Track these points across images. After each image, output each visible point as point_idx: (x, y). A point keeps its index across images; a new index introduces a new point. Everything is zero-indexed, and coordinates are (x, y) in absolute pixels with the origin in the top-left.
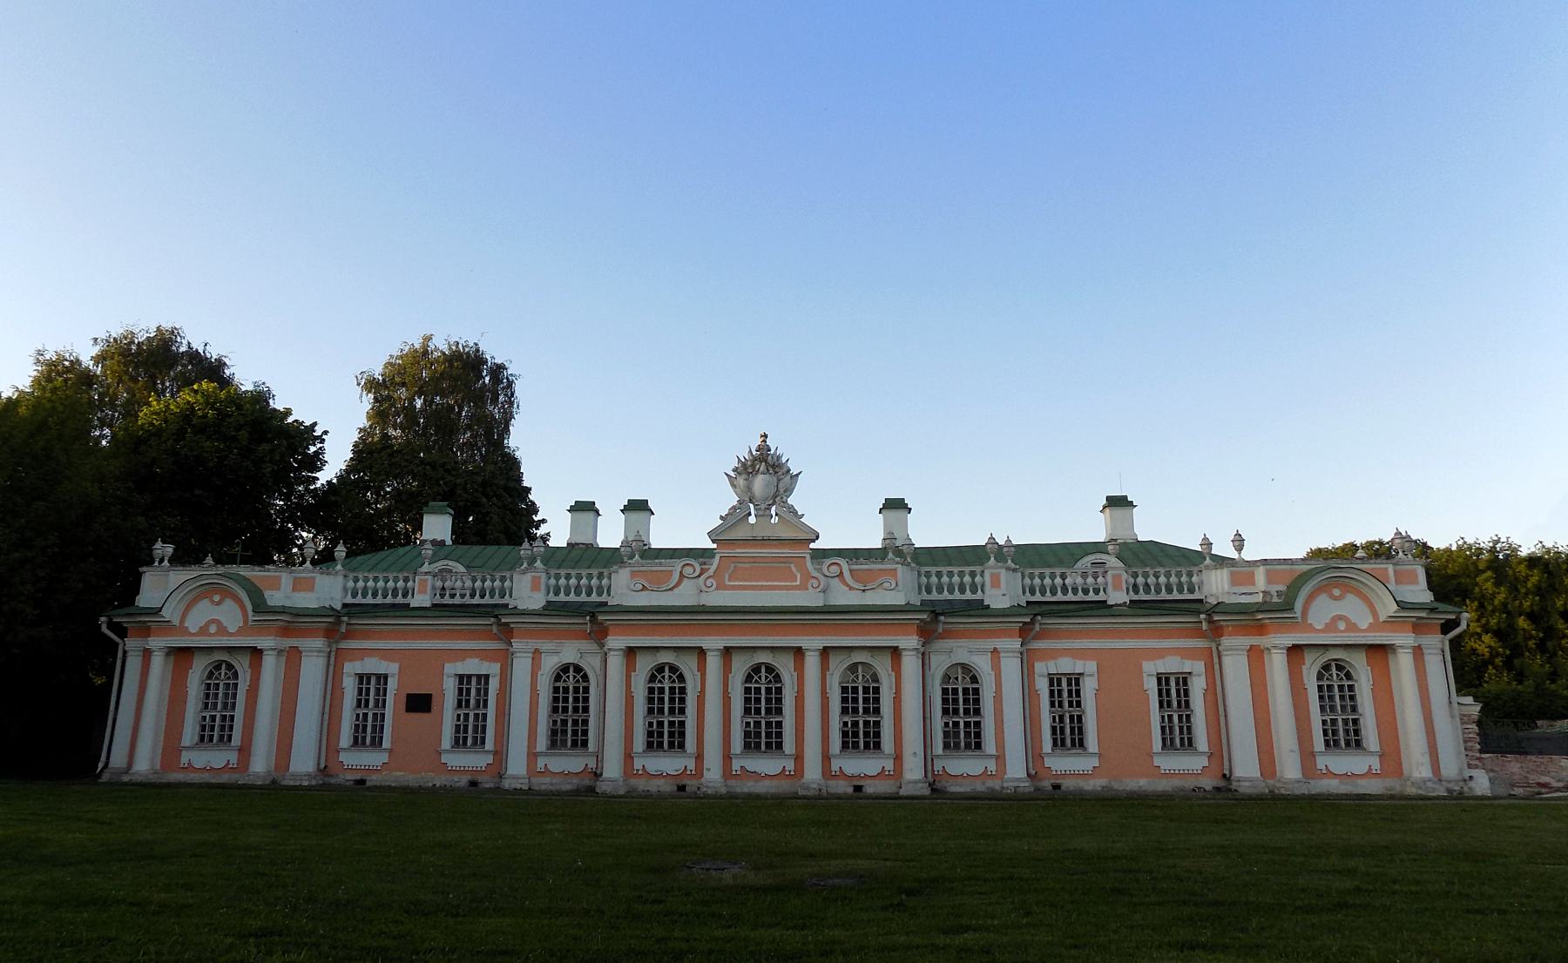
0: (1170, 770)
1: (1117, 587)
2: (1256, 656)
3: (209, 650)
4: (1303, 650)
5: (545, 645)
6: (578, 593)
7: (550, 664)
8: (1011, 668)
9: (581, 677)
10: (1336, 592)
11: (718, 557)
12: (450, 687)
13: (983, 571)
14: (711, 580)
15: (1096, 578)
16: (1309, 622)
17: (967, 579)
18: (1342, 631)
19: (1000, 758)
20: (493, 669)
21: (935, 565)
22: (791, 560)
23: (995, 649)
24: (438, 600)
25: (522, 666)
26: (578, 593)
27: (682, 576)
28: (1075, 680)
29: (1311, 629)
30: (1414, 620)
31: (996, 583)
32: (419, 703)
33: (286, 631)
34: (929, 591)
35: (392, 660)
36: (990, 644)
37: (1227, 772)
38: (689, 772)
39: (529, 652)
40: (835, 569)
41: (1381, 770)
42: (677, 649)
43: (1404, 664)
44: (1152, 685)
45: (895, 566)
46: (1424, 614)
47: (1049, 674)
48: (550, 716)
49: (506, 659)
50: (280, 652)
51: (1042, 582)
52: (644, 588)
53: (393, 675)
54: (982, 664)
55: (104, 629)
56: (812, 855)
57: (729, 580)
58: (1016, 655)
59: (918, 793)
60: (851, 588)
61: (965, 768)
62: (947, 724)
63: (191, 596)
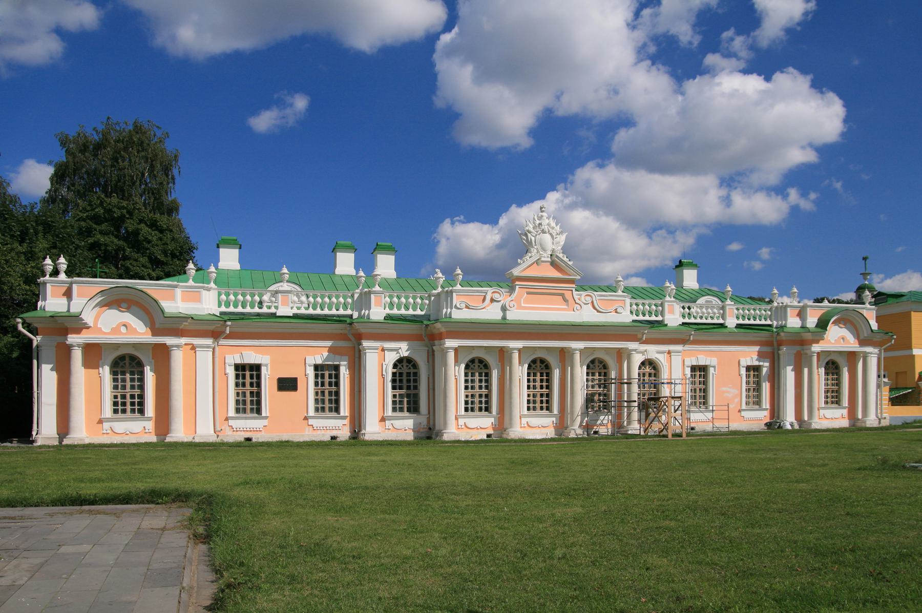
1: (731, 316)
9: (412, 366)
12: (311, 372)
23: (669, 351)
29: (829, 342)
32: (287, 384)
40: (588, 298)
45: (624, 298)
48: (419, 392)
53: (266, 365)
54: (662, 359)
55: (20, 327)
58: (876, 356)
60: (598, 311)
62: (394, 396)
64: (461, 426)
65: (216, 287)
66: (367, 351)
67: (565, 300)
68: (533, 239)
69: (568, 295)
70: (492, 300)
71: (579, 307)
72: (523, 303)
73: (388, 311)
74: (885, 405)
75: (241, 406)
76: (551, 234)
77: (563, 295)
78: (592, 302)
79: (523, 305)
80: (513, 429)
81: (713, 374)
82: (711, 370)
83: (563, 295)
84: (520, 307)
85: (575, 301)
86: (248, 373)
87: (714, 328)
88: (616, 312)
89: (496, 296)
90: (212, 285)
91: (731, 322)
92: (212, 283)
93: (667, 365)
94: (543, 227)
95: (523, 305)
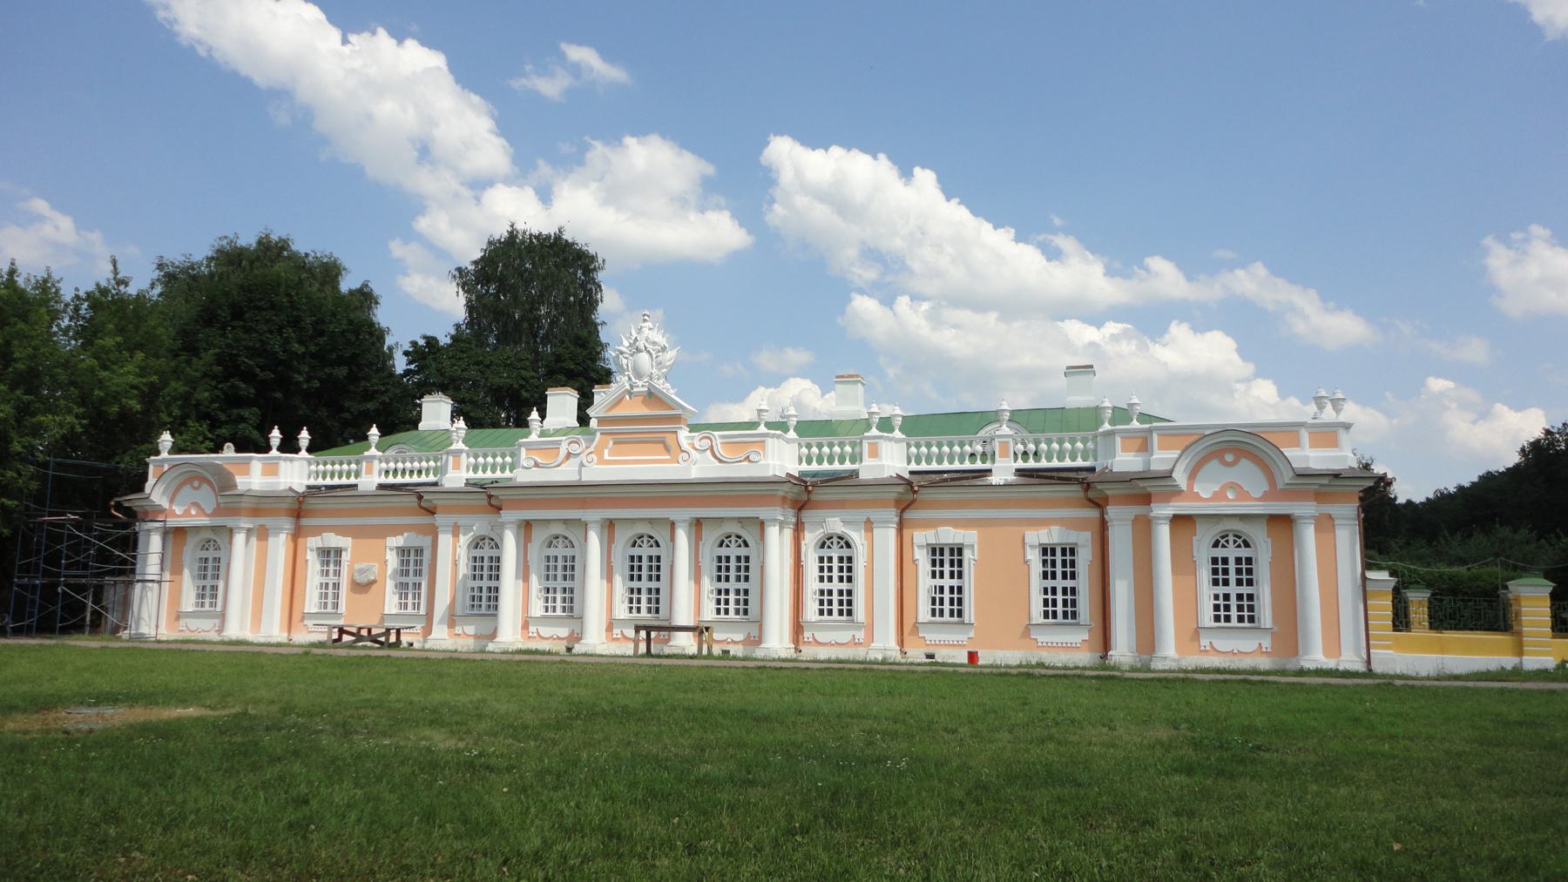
0: (1057, 643)
2: (1144, 528)
3: (197, 529)
4: (1195, 522)
5: (463, 520)
6: (820, 462)
7: (464, 540)
8: (887, 537)
10: (1229, 458)
11: (598, 434)
13: (861, 442)
14: (593, 456)
15: (1073, 444)
16: (1195, 491)
17: (848, 449)
18: (1232, 500)
19: (870, 628)
20: (425, 541)
21: (1068, 430)
22: (667, 435)
24: (383, 480)
25: (445, 540)
26: (831, 462)
27: (569, 455)
28: (958, 550)
29: (1197, 497)
30: (1317, 487)
31: (874, 453)
33: (255, 512)
34: (809, 462)
35: (344, 535)
36: (861, 514)
37: (384, 630)
38: (576, 635)
39: (449, 526)
40: (706, 443)
41: (1272, 648)
42: (740, 520)
43: (1308, 536)
44: (1034, 557)
45: (763, 439)
46: (1325, 481)
47: (928, 545)
49: (434, 532)
50: (249, 531)
51: (831, 451)
52: (537, 465)
54: (857, 537)
56: (767, 719)
57: (609, 455)
59: (789, 657)
60: (721, 461)
61: (730, 639)
63: (177, 482)
64: (1205, 647)
65: (904, 436)
66: (1114, 523)
67: (668, 450)
68: (625, 361)
69: (669, 438)
70: (569, 455)
71: (685, 456)
72: (609, 455)
73: (471, 475)
74: (1382, 628)
75: (1050, 609)
76: (649, 352)
77: (663, 442)
78: (711, 448)
79: (607, 457)
80: (1306, 657)
81: (970, 559)
82: (967, 554)
83: (663, 442)
84: (602, 461)
85: (680, 447)
86: (1059, 558)
87: (967, 478)
88: (750, 461)
89: (574, 448)
90: (897, 434)
91: (1003, 471)
92: (897, 431)
93: (865, 543)
94: (637, 344)
95: (607, 457)
